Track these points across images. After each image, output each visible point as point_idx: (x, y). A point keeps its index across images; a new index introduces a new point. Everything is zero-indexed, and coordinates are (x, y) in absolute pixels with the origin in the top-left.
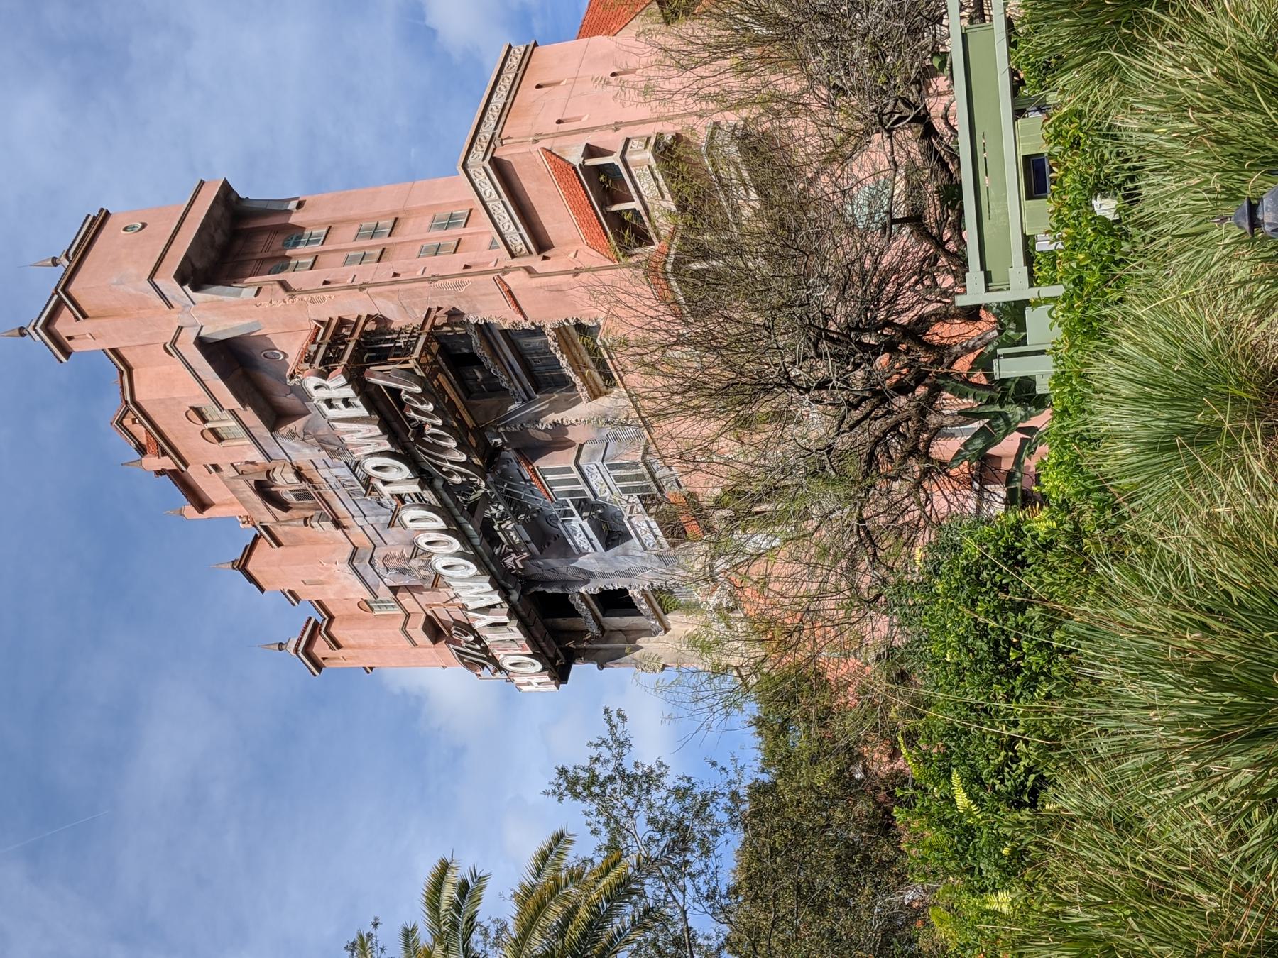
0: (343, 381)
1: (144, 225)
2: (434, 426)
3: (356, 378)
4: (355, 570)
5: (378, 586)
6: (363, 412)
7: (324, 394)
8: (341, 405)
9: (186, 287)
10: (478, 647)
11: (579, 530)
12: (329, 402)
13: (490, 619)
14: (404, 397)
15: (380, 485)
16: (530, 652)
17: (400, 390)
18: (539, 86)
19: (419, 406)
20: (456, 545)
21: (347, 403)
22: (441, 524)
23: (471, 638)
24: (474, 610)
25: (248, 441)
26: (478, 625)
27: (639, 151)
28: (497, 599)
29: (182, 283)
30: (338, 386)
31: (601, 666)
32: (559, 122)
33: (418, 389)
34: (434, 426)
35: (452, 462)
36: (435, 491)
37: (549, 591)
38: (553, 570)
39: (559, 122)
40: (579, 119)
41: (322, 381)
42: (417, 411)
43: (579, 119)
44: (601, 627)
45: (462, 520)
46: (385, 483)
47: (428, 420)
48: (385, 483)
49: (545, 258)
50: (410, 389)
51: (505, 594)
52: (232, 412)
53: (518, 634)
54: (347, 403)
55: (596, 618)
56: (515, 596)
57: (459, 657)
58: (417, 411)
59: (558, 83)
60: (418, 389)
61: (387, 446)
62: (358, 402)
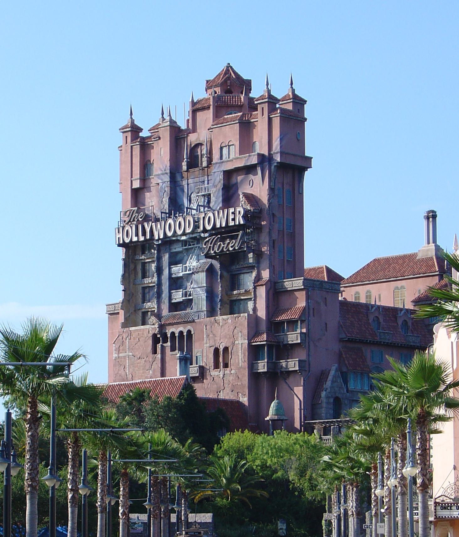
0: (242, 222)
1: (298, 140)
2: (223, 247)
5: (159, 178)
6: (231, 223)
8: (233, 217)
9: (276, 164)
11: (178, 271)
12: (233, 213)
13: (148, 230)
14: (234, 241)
19: (230, 245)
20: (179, 232)
21: (234, 220)
22: (188, 231)
25: (220, 161)
28: (157, 238)
32: (313, 309)
35: (210, 247)
40: (314, 315)
42: (229, 243)
43: (314, 315)
45: (188, 236)
46: (204, 218)
47: (226, 245)
48: (204, 218)
50: (236, 245)
51: (158, 240)
53: (142, 239)
54: (234, 220)
58: (229, 243)
59: (326, 305)
61: (218, 226)
62: (233, 224)
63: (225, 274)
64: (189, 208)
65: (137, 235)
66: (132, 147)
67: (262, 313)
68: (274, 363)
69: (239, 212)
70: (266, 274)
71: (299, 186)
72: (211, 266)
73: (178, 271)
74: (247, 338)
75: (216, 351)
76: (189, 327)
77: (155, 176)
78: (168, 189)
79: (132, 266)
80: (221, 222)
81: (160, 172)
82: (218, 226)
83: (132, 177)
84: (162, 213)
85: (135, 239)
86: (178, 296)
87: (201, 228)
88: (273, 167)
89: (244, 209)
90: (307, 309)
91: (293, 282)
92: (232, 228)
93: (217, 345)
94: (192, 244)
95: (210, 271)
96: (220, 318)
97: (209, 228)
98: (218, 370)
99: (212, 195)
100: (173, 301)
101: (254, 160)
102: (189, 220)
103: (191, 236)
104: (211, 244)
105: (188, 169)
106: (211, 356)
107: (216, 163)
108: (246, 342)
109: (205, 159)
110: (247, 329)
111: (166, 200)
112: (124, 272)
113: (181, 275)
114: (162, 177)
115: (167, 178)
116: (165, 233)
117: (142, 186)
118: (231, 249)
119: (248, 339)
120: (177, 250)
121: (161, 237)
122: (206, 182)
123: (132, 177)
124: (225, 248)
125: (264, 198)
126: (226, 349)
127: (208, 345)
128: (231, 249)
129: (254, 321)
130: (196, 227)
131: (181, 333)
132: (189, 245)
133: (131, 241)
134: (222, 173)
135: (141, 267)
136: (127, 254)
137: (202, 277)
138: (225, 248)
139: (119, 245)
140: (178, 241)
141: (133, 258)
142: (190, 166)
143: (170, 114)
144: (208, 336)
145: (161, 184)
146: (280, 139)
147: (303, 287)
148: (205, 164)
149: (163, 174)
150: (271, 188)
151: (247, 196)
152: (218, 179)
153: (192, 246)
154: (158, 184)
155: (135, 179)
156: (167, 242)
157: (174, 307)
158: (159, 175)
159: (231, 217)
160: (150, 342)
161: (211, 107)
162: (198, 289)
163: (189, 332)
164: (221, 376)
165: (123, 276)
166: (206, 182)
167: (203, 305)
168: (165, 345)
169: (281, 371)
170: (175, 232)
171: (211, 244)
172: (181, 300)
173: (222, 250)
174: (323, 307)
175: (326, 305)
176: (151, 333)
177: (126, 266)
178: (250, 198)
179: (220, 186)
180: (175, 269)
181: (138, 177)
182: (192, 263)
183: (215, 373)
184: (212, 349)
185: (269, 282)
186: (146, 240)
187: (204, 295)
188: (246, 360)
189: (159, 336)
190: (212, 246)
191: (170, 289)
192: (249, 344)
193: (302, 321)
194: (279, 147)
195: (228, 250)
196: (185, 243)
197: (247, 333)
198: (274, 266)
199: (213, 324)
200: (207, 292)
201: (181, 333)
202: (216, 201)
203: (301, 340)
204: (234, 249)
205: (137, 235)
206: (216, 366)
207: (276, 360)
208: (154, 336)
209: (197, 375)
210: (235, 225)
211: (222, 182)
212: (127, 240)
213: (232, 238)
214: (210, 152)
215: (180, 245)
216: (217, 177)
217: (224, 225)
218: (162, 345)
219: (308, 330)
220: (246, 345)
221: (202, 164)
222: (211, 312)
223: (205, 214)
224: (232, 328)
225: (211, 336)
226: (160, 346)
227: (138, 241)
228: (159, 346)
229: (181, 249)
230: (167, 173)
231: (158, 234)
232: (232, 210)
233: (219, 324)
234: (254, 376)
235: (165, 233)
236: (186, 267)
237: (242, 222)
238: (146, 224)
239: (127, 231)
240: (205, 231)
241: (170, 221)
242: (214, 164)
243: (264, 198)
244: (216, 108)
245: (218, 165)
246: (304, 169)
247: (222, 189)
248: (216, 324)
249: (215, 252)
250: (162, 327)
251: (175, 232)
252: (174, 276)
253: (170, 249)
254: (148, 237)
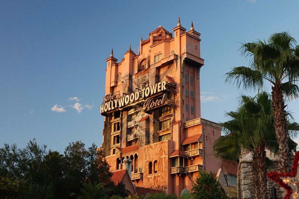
0: (165, 89)
2: (155, 104)
3: (164, 92)
4: (127, 76)
5: (123, 79)
6: (159, 91)
7: (162, 84)
8: (160, 87)
9: (184, 59)
10: (110, 99)
11: (131, 124)
12: (160, 85)
14: (161, 100)
15: (144, 89)
16: (109, 110)
17: (162, 99)
18: (213, 132)
19: (158, 102)
20: (132, 101)
21: (160, 88)
22: (136, 99)
23: (112, 99)
24: (118, 101)
25: (154, 63)
26: (115, 100)
27: (199, 152)
28: (120, 106)
29: (185, 58)
30: (164, 88)
31: (105, 122)
32: (207, 136)
33: (162, 103)
34: (155, 104)
35: (147, 105)
36: (142, 99)
37: (120, 115)
38: (125, 117)
39: (207, 136)
40: (207, 140)
41: (165, 84)
42: (158, 102)
43: (207, 140)
44: (112, 122)
45: (136, 103)
46: (145, 91)
47: (156, 103)
48: (145, 91)
49: (183, 130)
50: (162, 102)
51: (121, 108)
52: (160, 61)
53: (113, 108)
54: (160, 88)
55: (114, 122)
56: (120, 109)
57: (108, 95)
58: (158, 102)
59: (214, 136)
60: (162, 103)
61: (152, 93)
62: (160, 91)
63: (156, 121)
64: (137, 89)
65: (111, 107)
66: (111, 67)
67: (176, 138)
68: (184, 168)
69: (164, 83)
70: (178, 117)
71: (197, 74)
72: (149, 117)
73: (131, 124)
74: (167, 154)
75: (150, 163)
76: (136, 153)
77: (122, 78)
78: (128, 83)
79: (109, 126)
80: (153, 91)
81: (124, 76)
82: (152, 93)
83: (110, 82)
84: (124, 94)
85: (109, 109)
86: (131, 138)
87: (143, 97)
88: (182, 61)
89: (166, 82)
90: (203, 135)
91: (195, 121)
92: (159, 94)
93: (151, 160)
94: (139, 108)
95: (148, 120)
96: (152, 144)
97: (147, 95)
98: (151, 174)
99: (150, 81)
100: (129, 140)
101: (172, 58)
102: (137, 94)
103: (138, 102)
104: (148, 104)
105: (138, 72)
106: (148, 167)
107: (152, 65)
108: (167, 156)
109: (147, 65)
110: (167, 148)
111: (126, 89)
112: (105, 128)
113: (133, 126)
114: (125, 78)
115: (128, 78)
116: (124, 103)
117: (116, 85)
118: (158, 104)
119: (168, 155)
120: (131, 113)
121: (123, 105)
122: (147, 77)
123: (110, 82)
124: (155, 104)
125: (178, 80)
126: (156, 162)
127: (146, 161)
128: (158, 104)
129: (171, 144)
130: (140, 96)
131: (132, 156)
132: (138, 110)
133: (108, 111)
134: (155, 69)
135: (113, 126)
136: (107, 119)
137: (143, 123)
138: (155, 104)
139: (104, 114)
140: (131, 108)
141: (110, 122)
142: (139, 70)
143: (130, 48)
144: (146, 155)
145: (124, 82)
146: (187, 46)
147: (200, 123)
148: (147, 68)
149: (125, 76)
150: (182, 72)
151: (167, 77)
152: (153, 72)
153: (139, 110)
154: (123, 82)
155: (113, 82)
156: (127, 109)
157: (129, 143)
158: (124, 77)
159: (159, 87)
160: (116, 163)
161: (151, 41)
162: (141, 131)
163: (136, 155)
164: (153, 177)
165: (104, 130)
166: (147, 77)
167: (144, 140)
168: (122, 164)
169: (187, 172)
170: (130, 101)
171: (148, 104)
172: (133, 139)
173: (154, 106)
174: (212, 136)
175: (214, 136)
176: (116, 158)
177: (106, 125)
178: (169, 78)
179: (154, 76)
180: (129, 123)
181: (114, 80)
182: (138, 118)
183: (149, 176)
184: (148, 163)
185: (180, 123)
186: (115, 109)
187: (143, 133)
188: (167, 167)
189: (120, 159)
190: (148, 105)
191: (127, 134)
192: (169, 157)
193: (200, 142)
194: (186, 50)
195: (157, 106)
196: (135, 107)
197: (167, 151)
198: (183, 114)
199: (148, 148)
200: (146, 132)
201: (132, 156)
202: (152, 81)
203: (200, 153)
204: (161, 104)
205: (111, 107)
206: (150, 172)
207: (185, 166)
208: (118, 159)
209: (139, 178)
210: (161, 92)
211: (155, 73)
212: (106, 111)
213: (159, 99)
214: (149, 62)
215: (133, 110)
216: (153, 71)
217: (155, 92)
218: (121, 164)
219: (204, 148)
220: (167, 159)
221: (145, 68)
222: (148, 142)
223: (145, 89)
224: (159, 149)
225: (147, 155)
226: (120, 165)
227: (111, 110)
228: (120, 165)
229: (133, 112)
230: (127, 76)
231: (121, 104)
232: (160, 83)
233: (152, 148)
234: (172, 177)
235: (124, 103)
236: (136, 122)
237: (165, 89)
238: (115, 100)
239: (106, 105)
240: (145, 98)
241: (128, 96)
242: (151, 65)
243: (178, 80)
244: (153, 42)
245: (153, 66)
246: (200, 65)
247: (155, 77)
248: (150, 148)
249: (150, 108)
250: (121, 154)
251: (130, 101)
252: (129, 127)
253: (128, 114)
254: (116, 107)
